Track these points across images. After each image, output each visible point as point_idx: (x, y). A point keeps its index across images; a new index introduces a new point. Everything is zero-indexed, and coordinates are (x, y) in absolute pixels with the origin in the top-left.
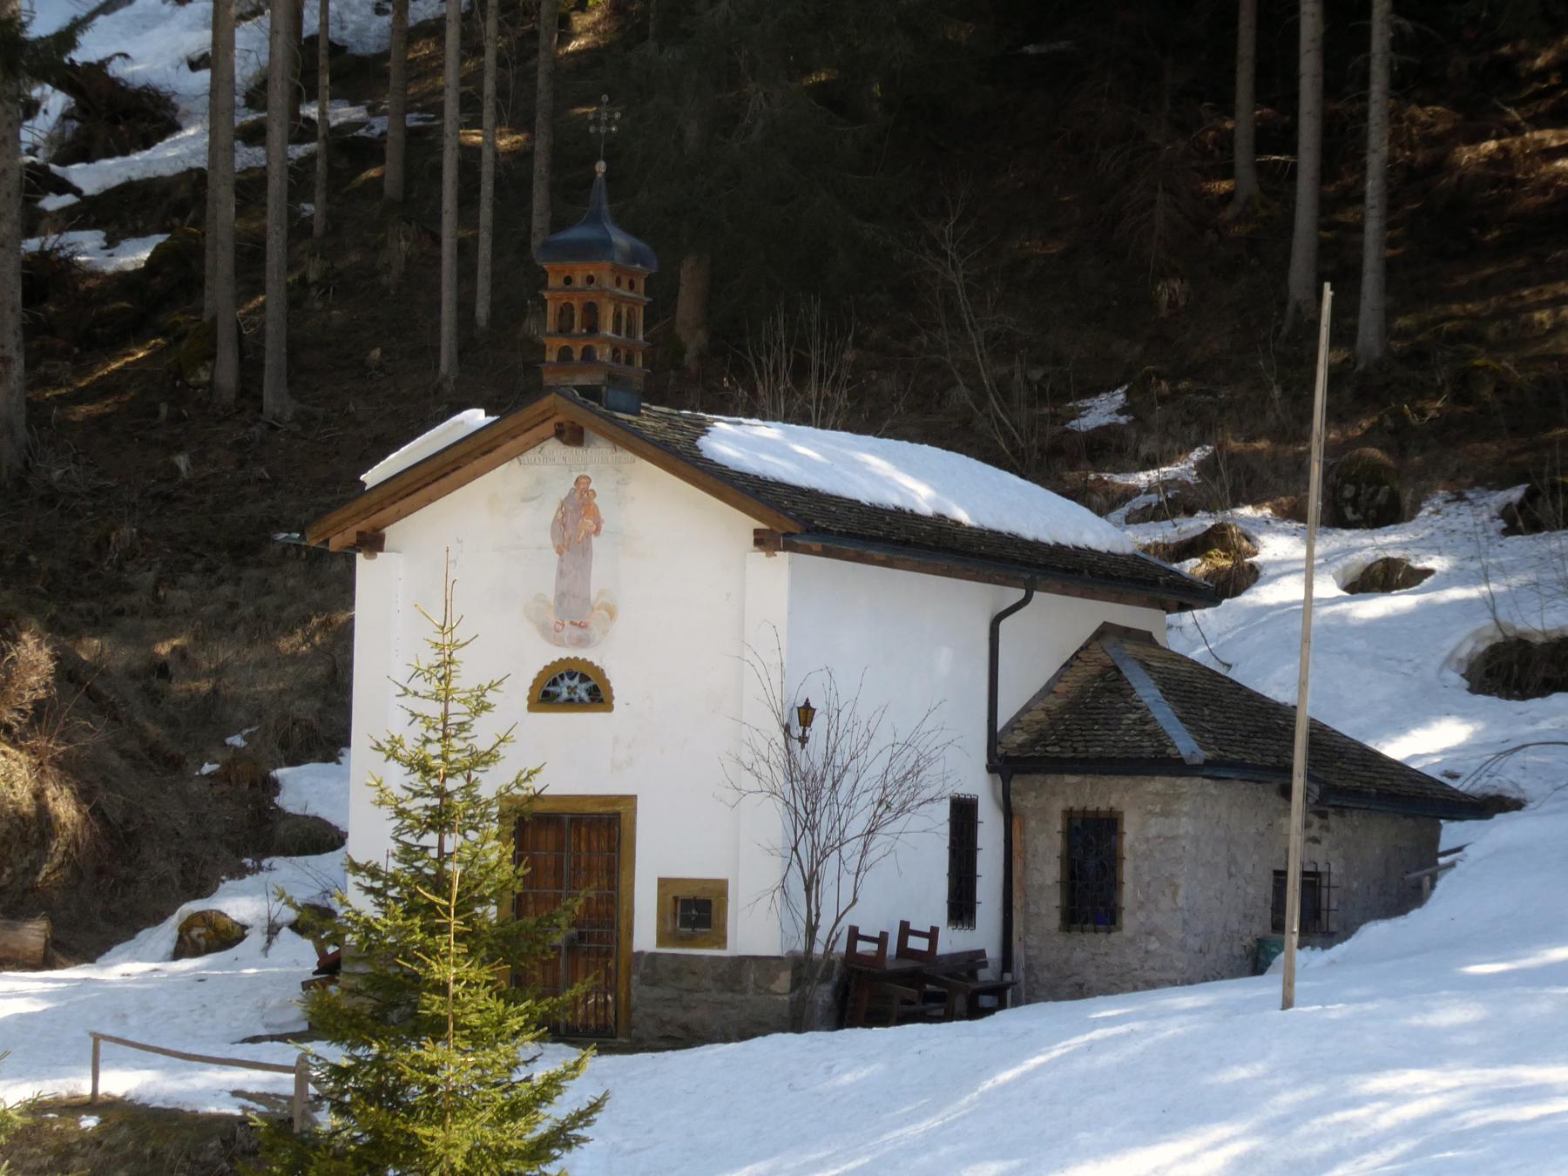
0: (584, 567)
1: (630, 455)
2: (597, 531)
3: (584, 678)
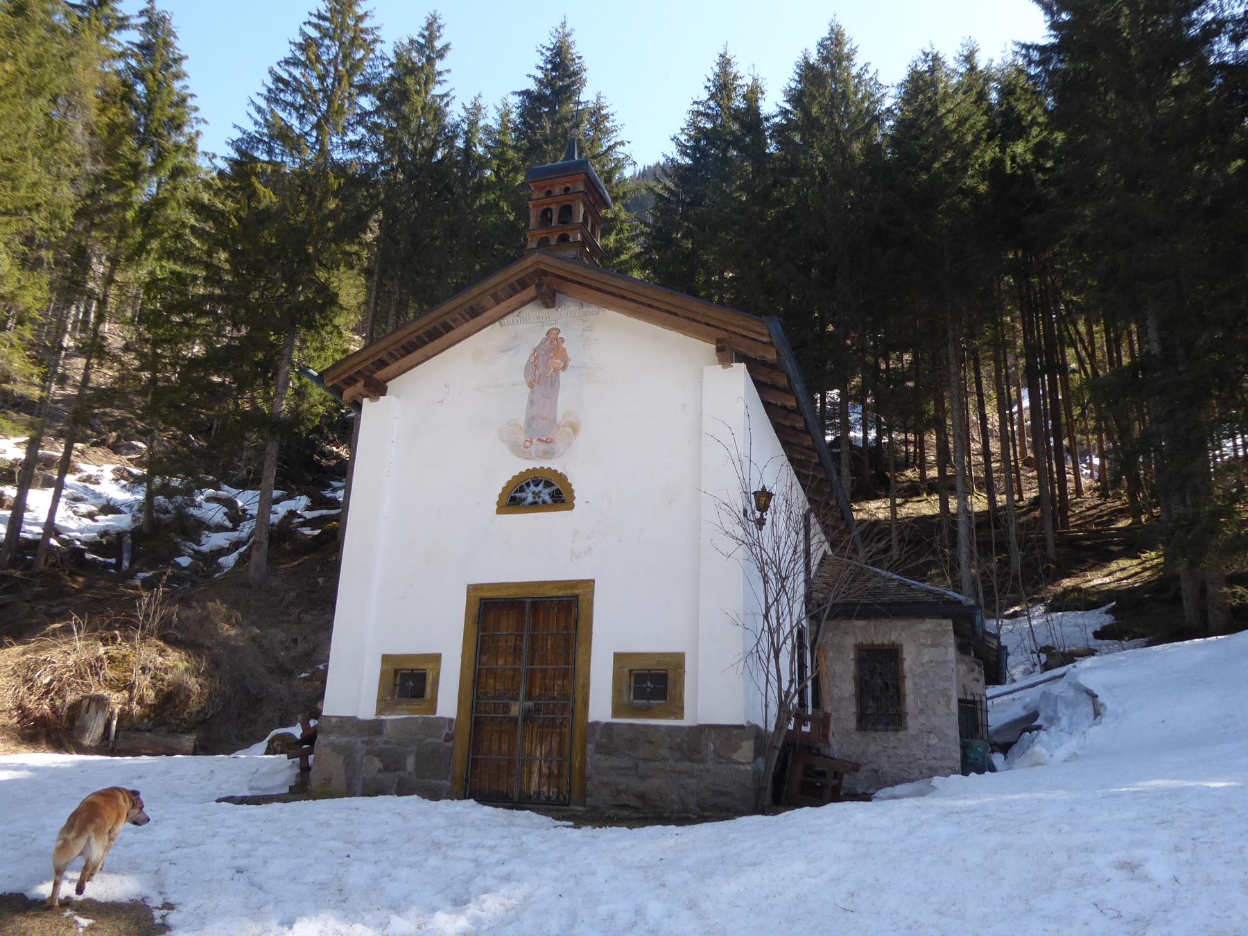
0: (552, 398)
1: (594, 309)
2: (564, 368)
3: (548, 484)
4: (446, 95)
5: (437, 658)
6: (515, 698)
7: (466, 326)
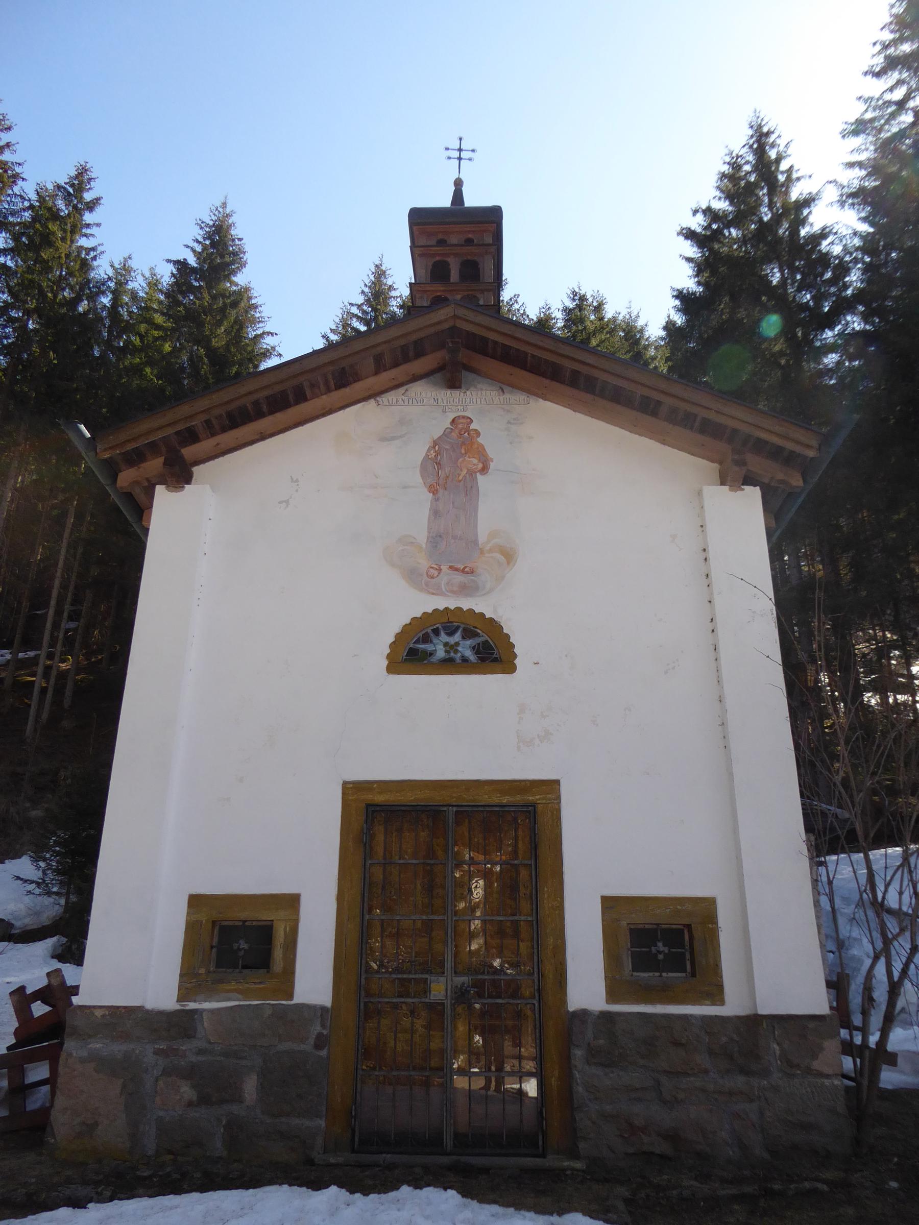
1: (521, 397)
2: (484, 470)
3: (469, 633)
4: (93, 249)
5: (292, 902)
7: (325, 400)
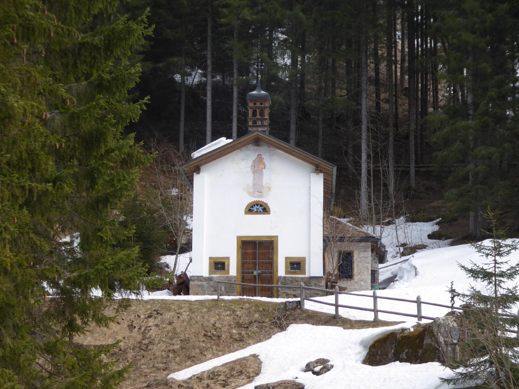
2: (265, 168)
3: (261, 206)
5: (228, 258)
6: (256, 269)
